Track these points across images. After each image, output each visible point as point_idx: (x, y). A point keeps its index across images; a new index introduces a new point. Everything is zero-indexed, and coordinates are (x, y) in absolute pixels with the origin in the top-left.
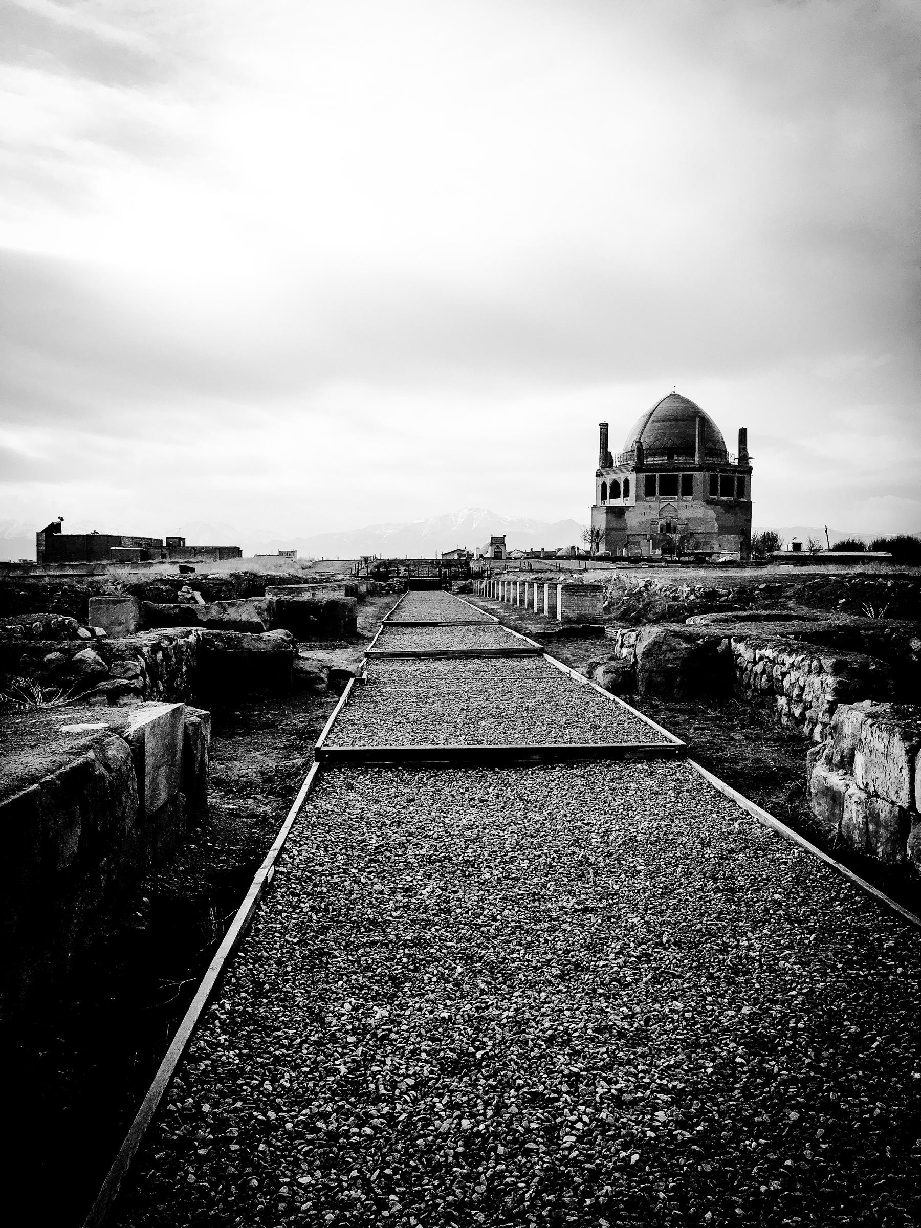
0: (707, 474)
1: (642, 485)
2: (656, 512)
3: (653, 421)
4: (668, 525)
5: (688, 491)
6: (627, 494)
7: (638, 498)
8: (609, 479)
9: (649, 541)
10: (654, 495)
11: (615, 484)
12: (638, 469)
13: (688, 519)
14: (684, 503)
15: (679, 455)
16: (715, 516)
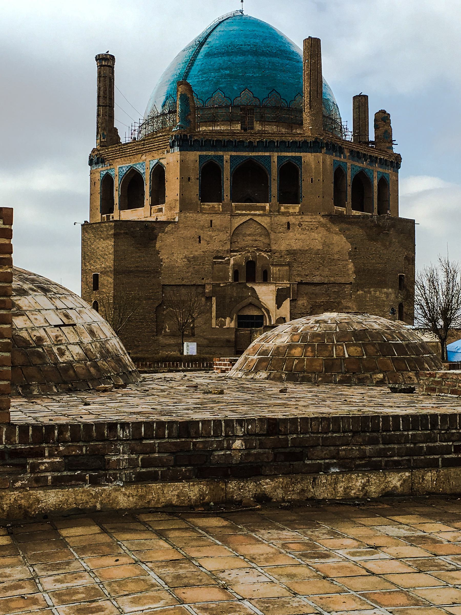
0: (329, 159)
1: (195, 175)
2: (225, 236)
3: (208, 55)
4: (251, 265)
5: (290, 192)
6: (158, 197)
7: (185, 205)
8: (118, 169)
9: (209, 299)
10: (219, 199)
11: (133, 180)
12: (184, 142)
13: (291, 252)
14: (284, 220)
15: (263, 120)
16: (348, 247)
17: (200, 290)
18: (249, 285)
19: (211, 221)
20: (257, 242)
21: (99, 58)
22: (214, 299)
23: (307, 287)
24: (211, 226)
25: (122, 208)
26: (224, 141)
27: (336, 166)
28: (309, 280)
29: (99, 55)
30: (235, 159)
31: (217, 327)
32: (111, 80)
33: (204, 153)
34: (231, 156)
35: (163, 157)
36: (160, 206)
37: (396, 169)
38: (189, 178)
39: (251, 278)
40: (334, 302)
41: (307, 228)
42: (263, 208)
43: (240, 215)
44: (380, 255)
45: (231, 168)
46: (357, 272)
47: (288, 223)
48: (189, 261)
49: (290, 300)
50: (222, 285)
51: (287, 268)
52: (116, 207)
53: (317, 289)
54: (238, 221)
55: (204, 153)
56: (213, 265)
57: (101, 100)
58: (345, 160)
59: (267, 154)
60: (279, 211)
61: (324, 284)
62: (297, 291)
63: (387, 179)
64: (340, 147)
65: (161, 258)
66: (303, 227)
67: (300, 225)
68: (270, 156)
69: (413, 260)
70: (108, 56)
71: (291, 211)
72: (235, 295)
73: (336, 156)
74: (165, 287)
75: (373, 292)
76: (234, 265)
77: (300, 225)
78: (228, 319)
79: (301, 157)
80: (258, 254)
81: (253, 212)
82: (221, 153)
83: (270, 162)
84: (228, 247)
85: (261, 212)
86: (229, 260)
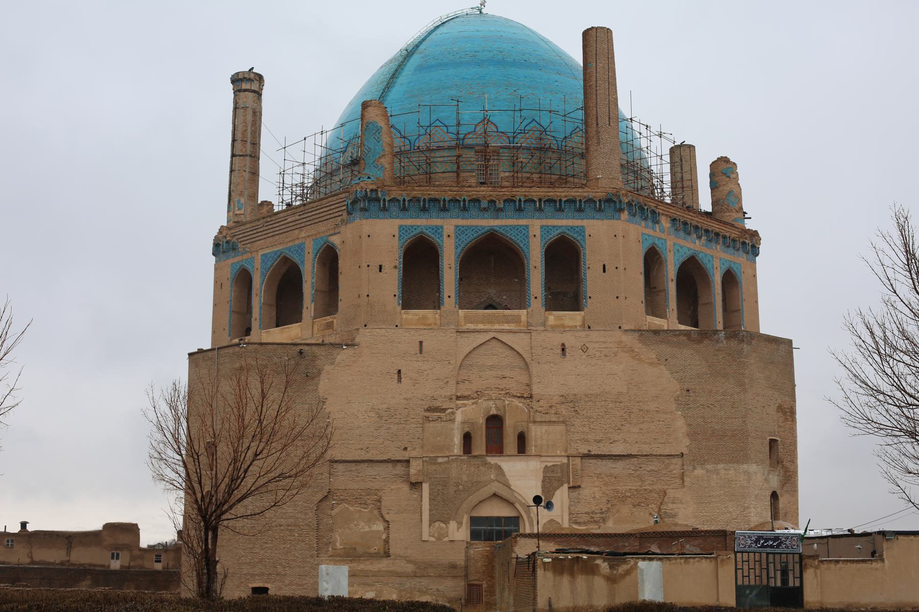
3: (421, 68)
4: (495, 422)
9: (416, 485)
10: (437, 304)
17: (400, 469)
18: (492, 460)
19: (421, 343)
20: (505, 381)
21: (237, 80)
22: (426, 487)
23: (599, 462)
24: (421, 352)
25: (265, 326)
26: (444, 200)
27: (647, 245)
28: (604, 449)
29: (238, 73)
30: (463, 232)
31: (432, 539)
32: (257, 115)
33: (409, 222)
34: (457, 227)
35: (337, 231)
36: (329, 319)
37: (751, 256)
38: (381, 267)
39: (496, 446)
40: (651, 491)
41: (598, 354)
42: (517, 320)
43: (474, 331)
44: (734, 403)
45: (456, 248)
46: (693, 435)
47: (563, 345)
48: (380, 417)
49: (569, 488)
50: (440, 460)
51: (561, 428)
52: (255, 325)
53: (618, 467)
54: (469, 343)
55: (409, 222)
56: (423, 424)
57: (238, 145)
58: (663, 236)
59: (523, 222)
60: (544, 324)
62: (582, 470)
64: (653, 212)
65: (327, 411)
66: (590, 352)
68: (527, 226)
69: (792, 412)
70: (252, 76)
71: (568, 322)
72: (465, 478)
73: (646, 227)
74: (335, 465)
75: (723, 472)
76: (463, 423)
77: (584, 349)
78: (453, 525)
79: (583, 227)
80: (507, 402)
81: (497, 327)
82: (437, 222)
83: (527, 237)
84: (451, 390)
85: (512, 327)
86: (453, 413)
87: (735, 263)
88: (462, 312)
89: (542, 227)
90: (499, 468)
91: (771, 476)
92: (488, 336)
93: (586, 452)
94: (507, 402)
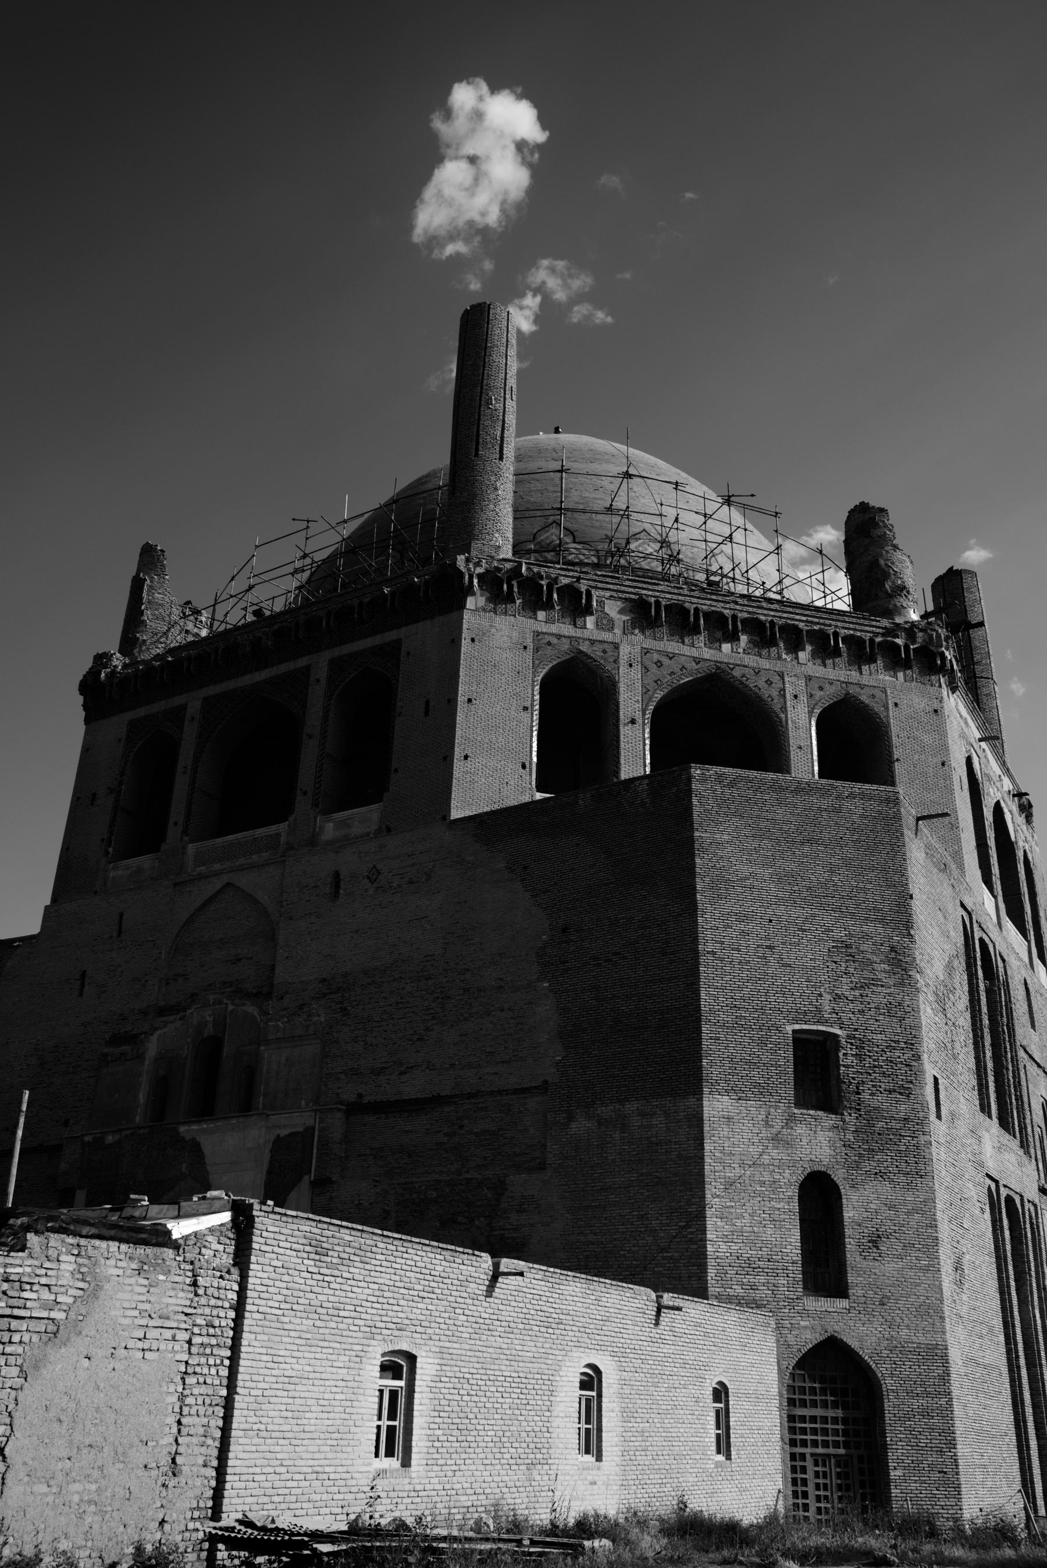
19: (121, 915)
33: (142, 712)
38: (94, 795)
47: (337, 875)
49: (311, 1183)
50: (110, 1139)
58: (607, 636)
59: (302, 662)
60: (312, 842)
61: (436, 1101)
63: (877, 708)
67: (373, 877)
77: (373, 877)
79: (398, 642)
80: (230, 1008)
82: (178, 700)
87: (862, 687)
88: (191, 849)
89: (332, 662)
90: (196, 1148)
91: (800, 1130)
92: (218, 884)
93: (353, 1098)
94: (230, 1008)
